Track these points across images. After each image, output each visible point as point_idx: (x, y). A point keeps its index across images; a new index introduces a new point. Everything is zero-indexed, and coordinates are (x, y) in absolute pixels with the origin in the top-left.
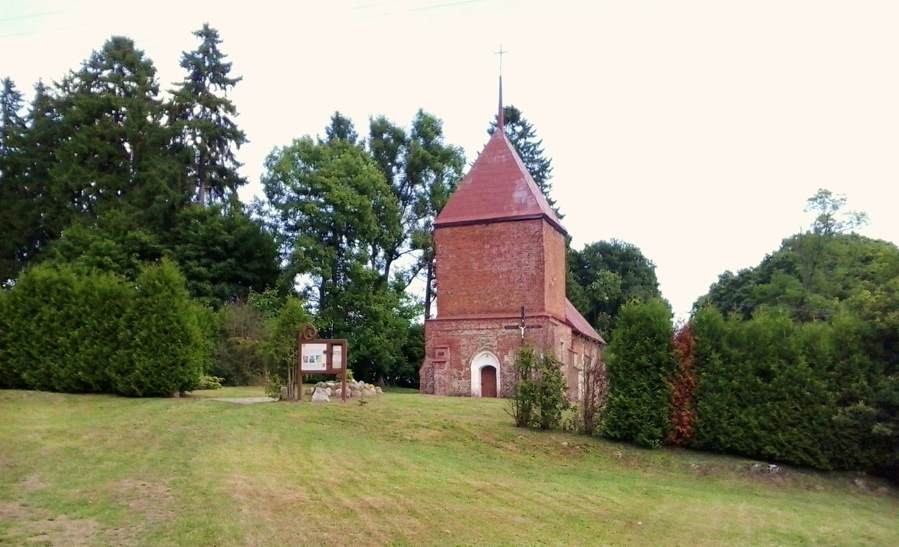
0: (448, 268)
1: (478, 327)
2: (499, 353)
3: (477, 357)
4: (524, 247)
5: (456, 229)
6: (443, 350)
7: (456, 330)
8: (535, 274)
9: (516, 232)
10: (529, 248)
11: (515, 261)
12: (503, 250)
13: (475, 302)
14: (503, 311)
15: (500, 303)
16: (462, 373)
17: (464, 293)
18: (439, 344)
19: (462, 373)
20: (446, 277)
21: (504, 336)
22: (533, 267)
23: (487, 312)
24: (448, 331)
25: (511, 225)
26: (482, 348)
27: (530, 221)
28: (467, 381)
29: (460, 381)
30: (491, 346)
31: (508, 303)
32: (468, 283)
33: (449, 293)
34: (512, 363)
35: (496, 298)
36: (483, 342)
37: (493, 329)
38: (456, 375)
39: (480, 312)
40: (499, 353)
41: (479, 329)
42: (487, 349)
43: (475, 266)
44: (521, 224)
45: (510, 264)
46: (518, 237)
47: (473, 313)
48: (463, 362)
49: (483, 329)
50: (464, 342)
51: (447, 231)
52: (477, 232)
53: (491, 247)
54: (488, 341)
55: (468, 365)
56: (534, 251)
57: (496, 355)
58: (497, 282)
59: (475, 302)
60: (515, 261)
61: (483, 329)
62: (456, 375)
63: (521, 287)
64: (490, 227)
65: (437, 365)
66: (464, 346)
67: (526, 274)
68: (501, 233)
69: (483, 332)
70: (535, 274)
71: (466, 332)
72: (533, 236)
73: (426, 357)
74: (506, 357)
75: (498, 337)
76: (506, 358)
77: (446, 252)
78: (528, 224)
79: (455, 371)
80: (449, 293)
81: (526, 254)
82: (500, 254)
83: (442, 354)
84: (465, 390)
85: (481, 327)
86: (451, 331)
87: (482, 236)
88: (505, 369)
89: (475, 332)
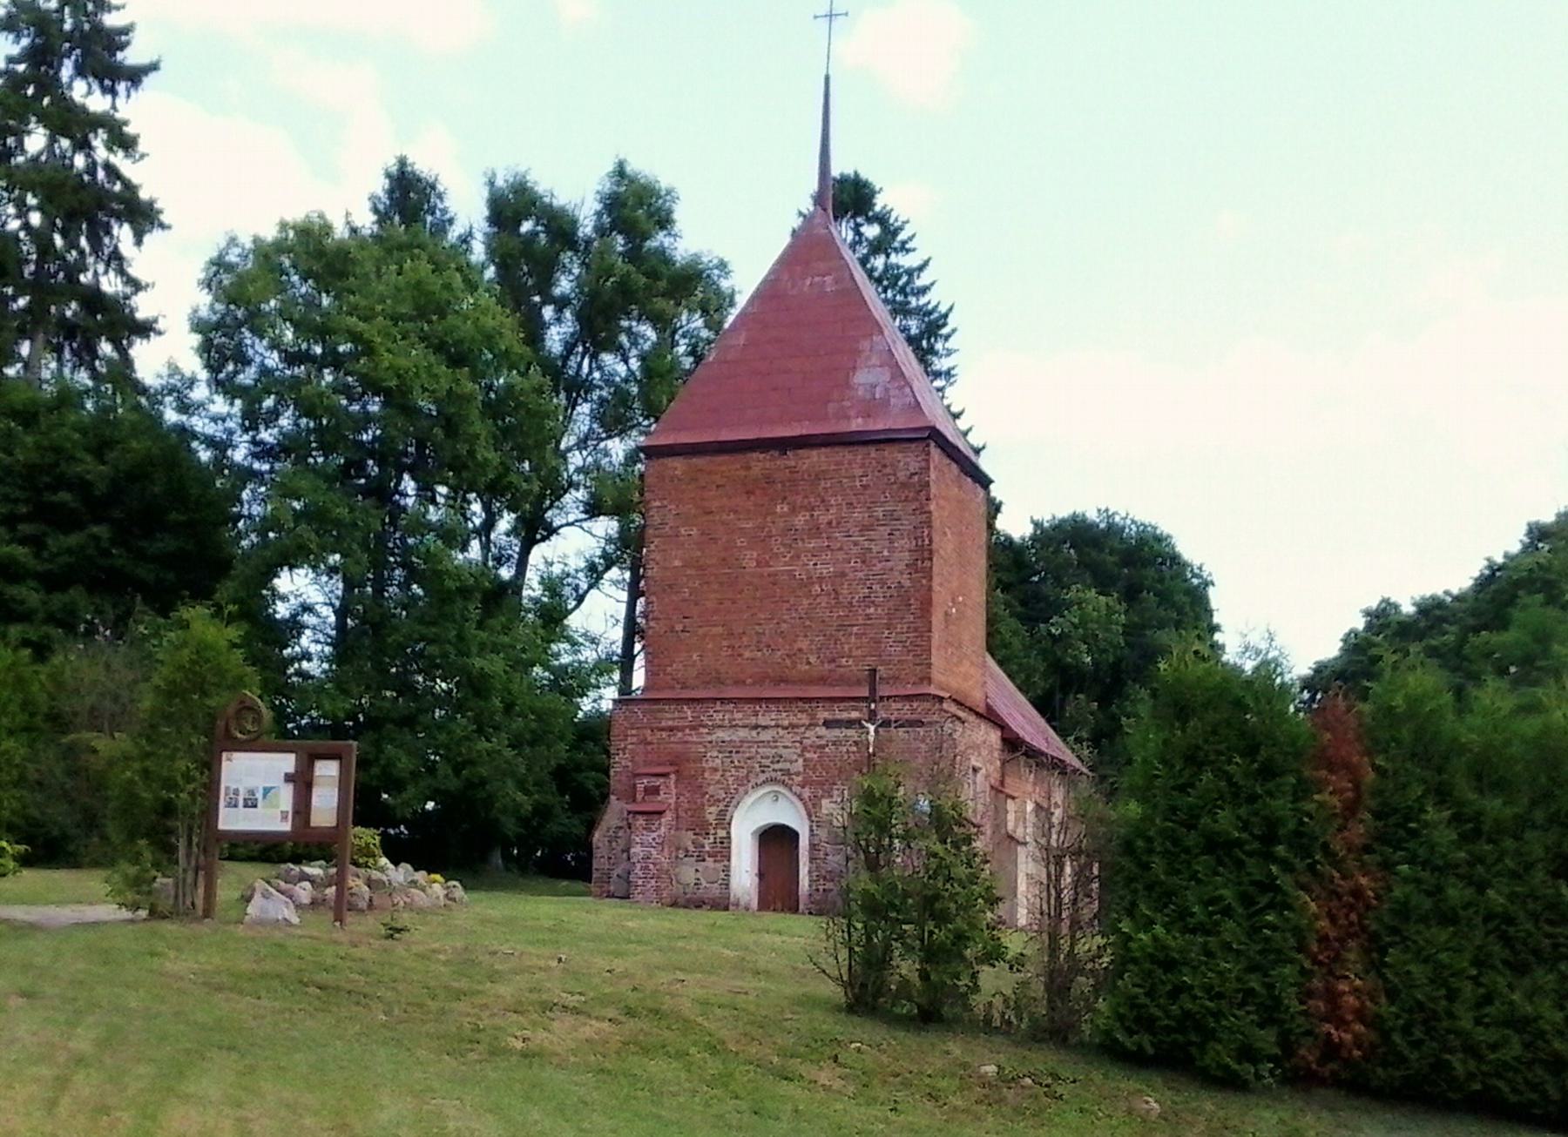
0: (677, 563)
1: (753, 720)
2: (806, 793)
3: (749, 800)
4: (879, 512)
5: (699, 461)
6: (659, 781)
7: (693, 728)
8: (907, 583)
9: (859, 472)
10: (891, 516)
11: (855, 550)
12: (824, 519)
13: (747, 654)
14: (822, 680)
15: (812, 659)
16: (707, 844)
17: (720, 630)
18: (646, 764)
19: (707, 844)
20: (670, 586)
21: (823, 747)
22: (902, 566)
23: (782, 680)
24: (671, 729)
25: (844, 454)
26: (762, 777)
27: (897, 447)
28: (720, 866)
29: (701, 866)
30: (787, 772)
31: (833, 660)
32: (728, 604)
33: (679, 627)
34: (840, 819)
35: (803, 644)
36: (766, 762)
37: (793, 726)
38: (691, 848)
39: (761, 680)
40: (806, 793)
41: (756, 727)
42: (773, 781)
43: (749, 558)
44: (872, 451)
45: (840, 556)
46: (865, 487)
47: (739, 682)
48: (711, 813)
49: (765, 727)
50: (715, 759)
51: (678, 465)
52: (756, 470)
53: (794, 510)
54: (779, 758)
55: (724, 822)
56: (907, 524)
57: (800, 798)
58: (805, 602)
59: (747, 654)
60: (855, 550)
61: (765, 727)
62: (691, 848)
63: (868, 617)
64: (791, 459)
65: (641, 821)
66: (716, 770)
67: (882, 583)
68: (819, 476)
69: (766, 736)
70: (907, 583)
71: (721, 734)
72: (904, 485)
73: (613, 798)
74: (825, 802)
75: (804, 749)
76: (827, 806)
77: (670, 518)
78: (890, 453)
79: (688, 838)
80: (679, 627)
81: (884, 531)
82: (815, 530)
83: (655, 791)
84: (715, 890)
85: (762, 721)
86: (681, 729)
87: (769, 480)
88: (823, 834)
89: (743, 733)
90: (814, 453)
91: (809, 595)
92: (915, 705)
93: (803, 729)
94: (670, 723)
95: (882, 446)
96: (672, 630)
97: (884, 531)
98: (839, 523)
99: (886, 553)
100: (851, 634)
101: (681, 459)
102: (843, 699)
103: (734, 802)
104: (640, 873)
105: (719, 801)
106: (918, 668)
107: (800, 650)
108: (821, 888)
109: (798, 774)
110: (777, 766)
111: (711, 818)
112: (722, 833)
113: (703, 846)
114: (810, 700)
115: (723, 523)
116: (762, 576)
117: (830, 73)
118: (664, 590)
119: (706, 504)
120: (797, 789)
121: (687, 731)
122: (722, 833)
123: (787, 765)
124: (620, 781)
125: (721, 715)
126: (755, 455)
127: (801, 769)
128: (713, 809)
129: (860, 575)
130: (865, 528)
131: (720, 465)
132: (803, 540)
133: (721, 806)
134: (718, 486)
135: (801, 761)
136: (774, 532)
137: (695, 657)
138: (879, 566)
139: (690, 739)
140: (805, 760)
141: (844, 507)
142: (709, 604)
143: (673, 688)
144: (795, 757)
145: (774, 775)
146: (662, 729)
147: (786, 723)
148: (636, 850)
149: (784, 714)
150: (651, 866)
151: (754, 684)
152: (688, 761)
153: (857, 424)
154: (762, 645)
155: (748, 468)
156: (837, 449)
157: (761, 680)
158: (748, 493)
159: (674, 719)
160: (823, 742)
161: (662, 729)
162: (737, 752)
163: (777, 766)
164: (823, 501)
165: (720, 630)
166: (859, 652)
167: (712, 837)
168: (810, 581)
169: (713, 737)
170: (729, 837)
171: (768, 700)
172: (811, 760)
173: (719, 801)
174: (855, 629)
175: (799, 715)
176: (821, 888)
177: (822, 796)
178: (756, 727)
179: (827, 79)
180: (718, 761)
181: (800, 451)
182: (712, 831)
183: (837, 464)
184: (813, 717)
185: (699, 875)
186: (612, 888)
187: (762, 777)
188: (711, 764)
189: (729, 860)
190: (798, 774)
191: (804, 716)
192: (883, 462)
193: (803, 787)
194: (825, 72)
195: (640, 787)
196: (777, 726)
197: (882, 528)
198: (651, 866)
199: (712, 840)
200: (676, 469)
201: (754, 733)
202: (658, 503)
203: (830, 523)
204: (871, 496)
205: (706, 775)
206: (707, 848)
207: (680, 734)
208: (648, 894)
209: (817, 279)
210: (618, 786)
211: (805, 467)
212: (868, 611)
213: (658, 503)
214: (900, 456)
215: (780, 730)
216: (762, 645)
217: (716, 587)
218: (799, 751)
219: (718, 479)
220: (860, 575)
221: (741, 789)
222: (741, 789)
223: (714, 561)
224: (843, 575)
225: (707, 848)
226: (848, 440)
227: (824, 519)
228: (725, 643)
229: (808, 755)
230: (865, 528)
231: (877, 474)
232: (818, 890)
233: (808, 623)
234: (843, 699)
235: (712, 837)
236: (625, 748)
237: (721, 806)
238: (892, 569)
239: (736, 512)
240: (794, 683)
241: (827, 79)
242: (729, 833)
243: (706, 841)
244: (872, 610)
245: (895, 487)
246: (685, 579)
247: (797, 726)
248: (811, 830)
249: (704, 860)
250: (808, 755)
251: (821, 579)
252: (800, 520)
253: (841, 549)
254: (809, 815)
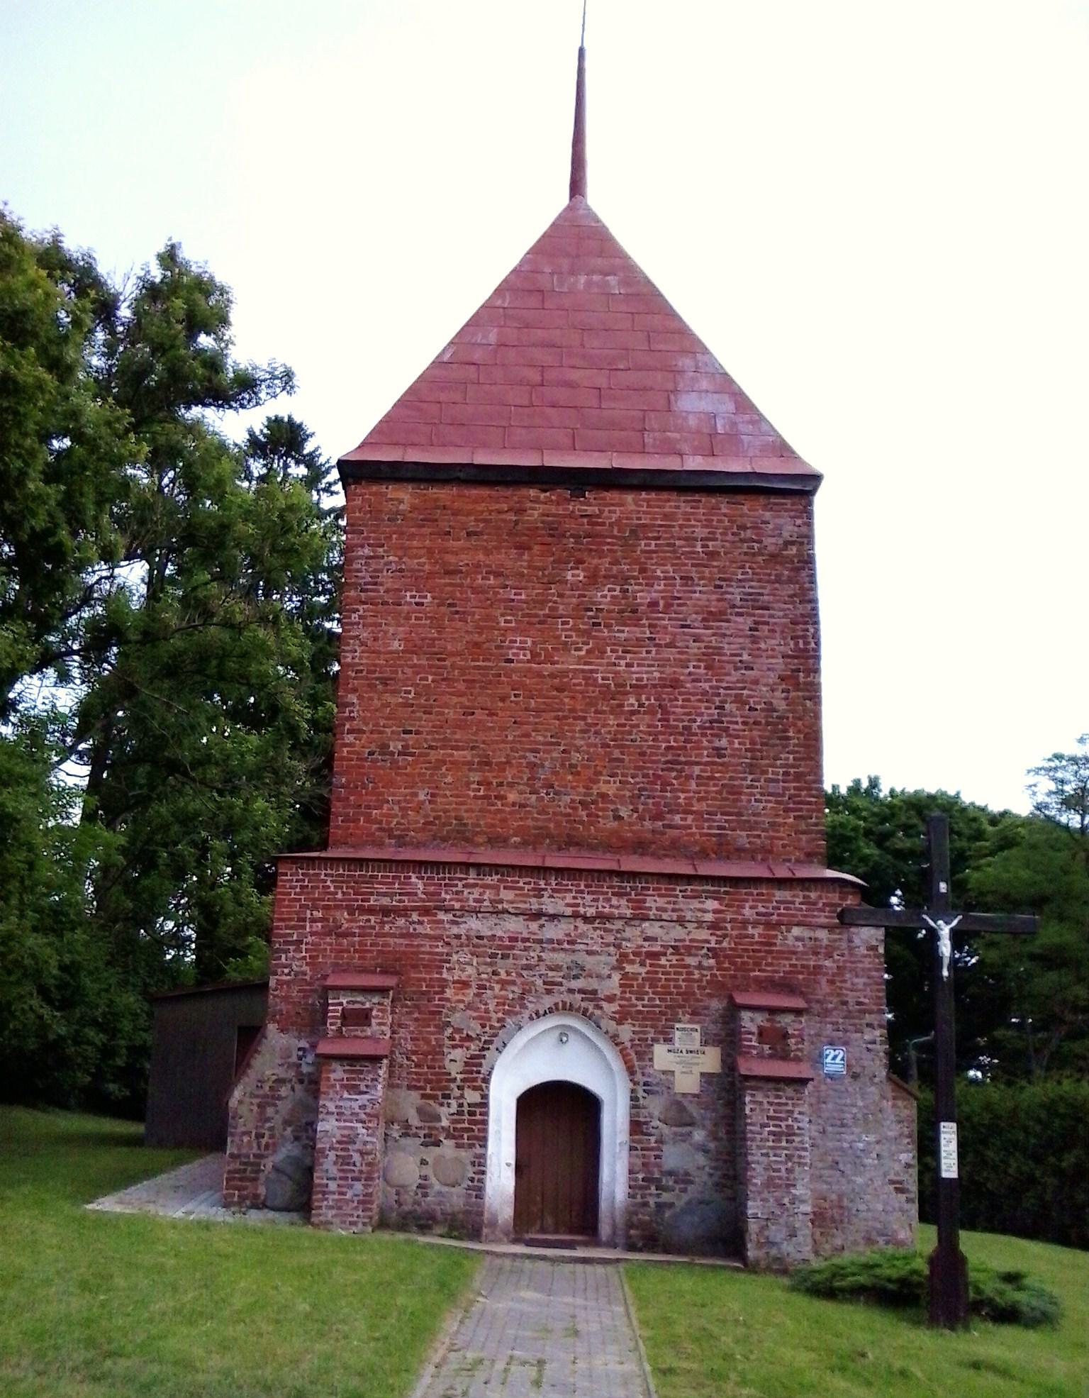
0: (396, 645)
1: (534, 905)
2: (626, 1032)
3: (520, 1040)
4: (736, 594)
5: (443, 494)
6: (368, 1002)
7: (425, 911)
8: (781, 705)
9: (700, 532)
10: (754, 603)
11: (695, 649)
12: (643, 597)
13: (512, 797)
14: (640, 847)
15: (624, 812)
16: (445, 1114)
17: (467, 755)
18: (339, 969)
19: (445, 1114)
20: (385, 682)
21: (654, 955)
22: (772, 678)
23: (571, 842)
24: (386, 911)
25: (678, 505)
26: (548, 1001)
27: (762, 500)
28: (465, 1155)
29: (432, 1154)
30: (591, 995)
31: (658, 816)
32: (480, 715)
33: (396, 746)
34: (687, 1083)
35: (610, 789)
36: (555, 976)
37: (604, 918)
38: (415, 1121)
39: (532, 840)
40: (626, 1032)
41: (537, 915)
42: (568, 1008)
43: (520, 647)
44: (724, 505)
45: (670, 654)
46: (712, 555)
47: (496, 841)
48: (455, 1060)
49: (553, 917)
50: (465, 966)
51: (403, 496)
52: (534, 515)
53: (593, 579)
54: (578, 971)
55: (477, 1077)
56: (778, 616)
57: (614, 1039)
58: (612, 721)
59: (512, 797)
60: (695, 649)
61: (553, 917)
62: (415, 1121)
63: (718, 752)
64: (591, 504)
65: (338, 1073)
66: (465, 984)
67: (739, 700)
68: (638, 532)
69: (554, 931)
70: (781, 705)
71: (474, 925)
72: (774, 558)
73: (272, 1028)
74: (660, 1050)
75: (623, 958)
76: (662, 1056)
77: (387, 579)
78: (750, 509)
79: (409, 1103)
80: (396, 746)
81: (745, 623)
82: (631, 614)
83: (363, 1017)
84: (456, 1199)
85: (550, 905)
86: (403, 912)
87: (554, 531)
88: (655, 1107)
89: (514, 925)
90: (629, 497)
91: (617, 710)
92: (813, 895)
93: (619, 924)
94: (385, 901)
95: (740, 498)
96: (384, 748)
97: (745, 623)
98: (668, 606)
99: (745, 657)
100: (689, 777)
101: (410, 487)
102: (689, 879)
103: (497, 1042)
104: (334, 1171)
105: (469, 1038)
106: (804, 837)
107: (604, 796)
108: (652, 1201)
109: (610, 999)
110: (575, 984)
111: (455, 1070)
112: (472, 1096)
113: (439, 1119)
114: (633, 875)
115: (475, 590)
116: (539, 675)
117: (585, 45)
118: (372, 687)
119: (451, 559)
120: (612, 1026)
121: (415, 917)
122: (472, 1096)
123: (593, 984)
124: (286, 999)
125: (476, 893)
126: (533, 492)
127: (618, 992)
128: (458, 1054)
129: (706, 686)
130: (711, 617)
131: (476, 502)
132: (608, 626)
133: (474, 1048)
134: (469, 534)
135: (616, 977)
136: (561, 609)
137: (422, 797)
138: (735, 676)
139: (420, 929)
140: (625, 976)
141: (678, 581)
142: (450, 714)
143: (380, 845)
144: (606, 972)
145: (568, 998)
146: (371, 911)
147: (591, 912)
148: (328, 1126)
149: (589, 897)
150: (356, 1157)
151: (525, 843)
152: (414, 967)
153: (695, 463)
154: (538, 784)
155: (521, 511)
156: (665, 495)
157: (532, 840)
158: (522, 547)
159: (391, 895)
160: (657, 948)
161: (371, 911)
162: (504, 957)
163: (575, 984)
164: (643, 570)
165: (467, 755)
166: (703, 806)
167: (454, 1103)
168: (621, 690)
169: (460, 930)
170: (484, 1104)
171: (560, 872)
172: (635, 976)
173: (469, 1038)
174: (697, 770)
175: (614, 901)
176: (652, 1201)
177: (655, 1040)
178: (537, 915)
179: (581, 52)
180: (470, 970)
181: (608, 495)
182: (457, 1093)
183: (666, 516)
184: (638, 904)
185: (428, 1171)
186: (262, 1190)
187: (548, 1001)
188: (457, 975)
189: (484, 1146)
190: (610, 999)
191: (623, 902)
192: (740, 521)
193: (620, 1022)
194: (580, 45)
195: (335, 1011)
196: (575, 915)
197: (740, 619)
198: (356, 1157)
199: (454, 1108)
200: (401, 501)
201: (534, 926)
202: (367, 551)
203: (653, 604)
204: (722, 570)
205: (449, 993)
206: (445, 1123)
207: (401, 922)
208: (347, 1209)
209: (596, 278)
210: (283, 1007)
211: (614, 517)
212: (717, 744)
213: (367, 551)
214: (768, 515)
215: (579, 923)
216: (538, 784)
217: (461, 686)
218: (613, 960)
219: (472, 525)
220: (706, 686)
221: (509, 1021)
222: (509, 1021)
223: (460, 646)
224: (675, 684)
225: (445, 1123)
226: (683, 483)
227: (643, 597)
228: (475, 777)
229: (629, 968)
230: (711, 617)
231: (730, 537)
232: (646, 1204)
233: (616, 754)
234: (689, 879)
235: (454, 1103)
236: (300, 942)
237: (474, 1048)
238: (756, 682)
239: (498, 575)
240: (592, 848)
241: (581, 52)
242: (485, 1096)
243: (444, 1111)
244: (724, 742)
245: (760, 559)
246: (409, 671)
247: (609, 918)
248: (634, 1098)
249: (437, 1144)
250: (629, 968)
251: (638, 688)
252: (604, 596)
253: (671, 645)
254: (631, 1071)
